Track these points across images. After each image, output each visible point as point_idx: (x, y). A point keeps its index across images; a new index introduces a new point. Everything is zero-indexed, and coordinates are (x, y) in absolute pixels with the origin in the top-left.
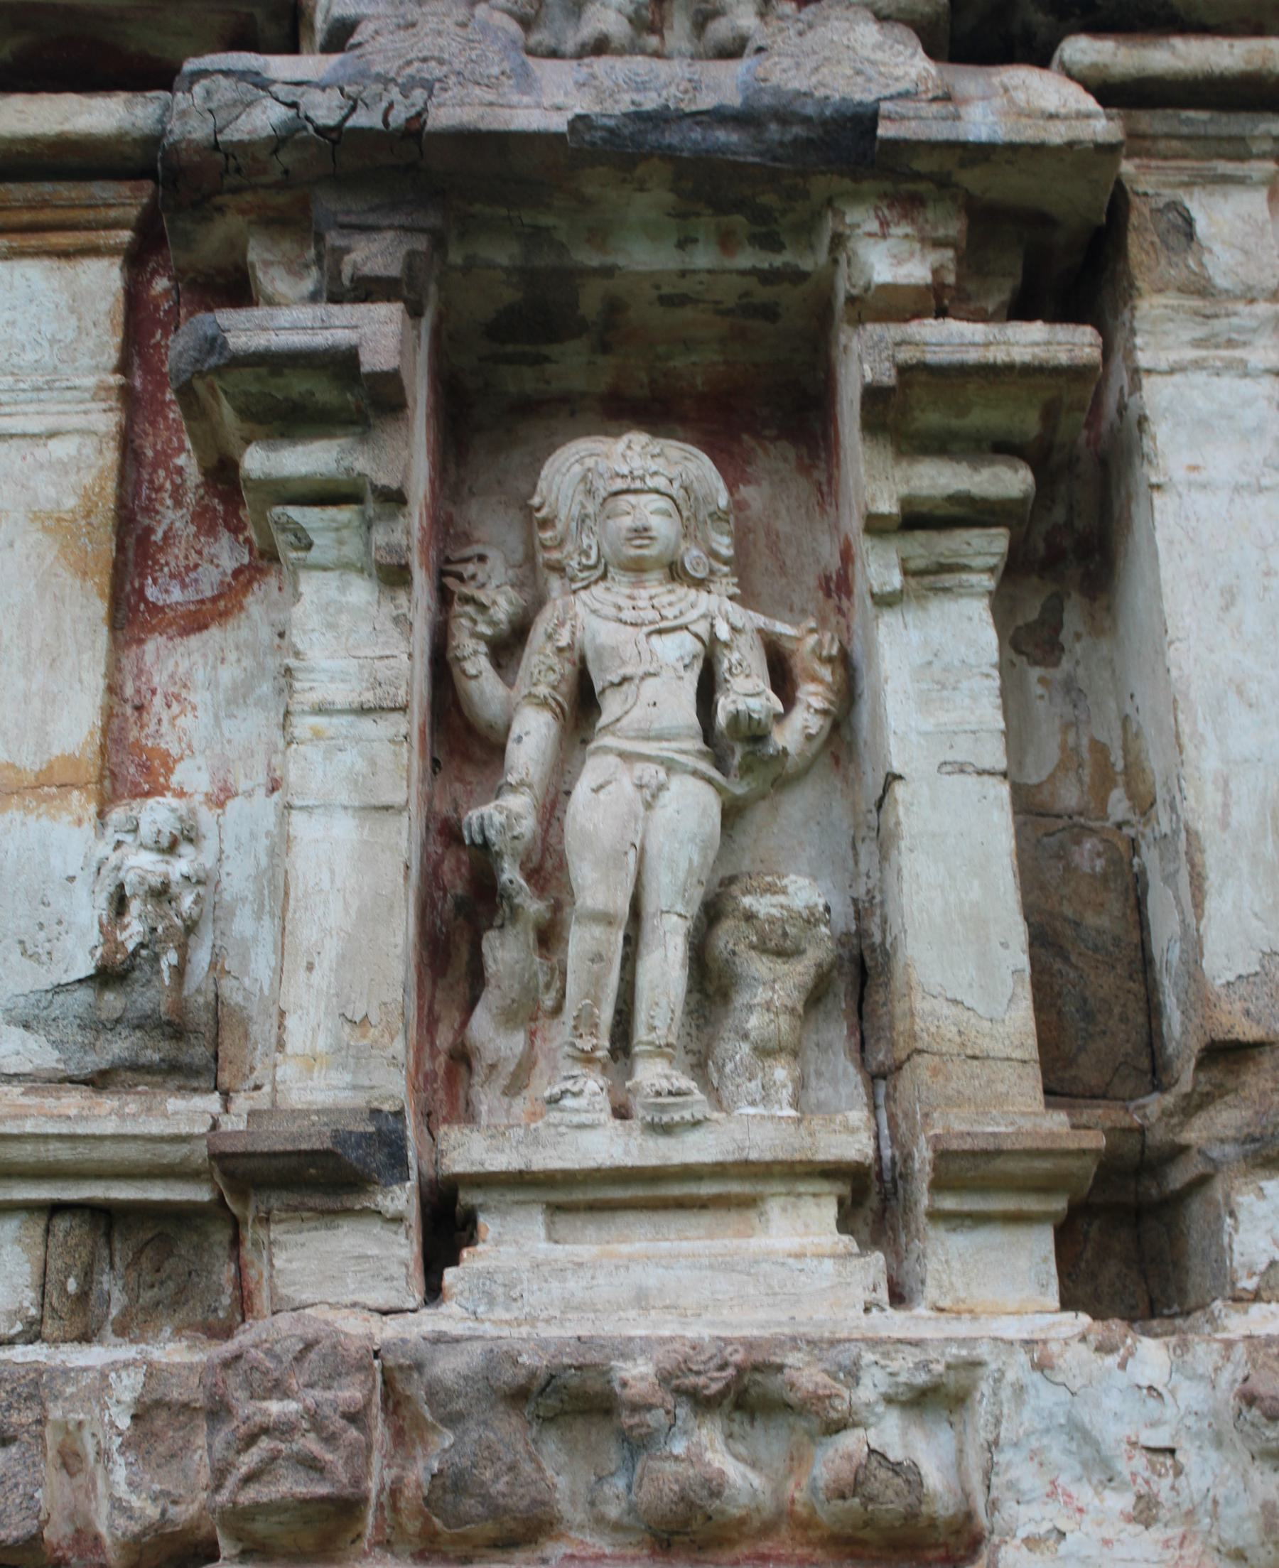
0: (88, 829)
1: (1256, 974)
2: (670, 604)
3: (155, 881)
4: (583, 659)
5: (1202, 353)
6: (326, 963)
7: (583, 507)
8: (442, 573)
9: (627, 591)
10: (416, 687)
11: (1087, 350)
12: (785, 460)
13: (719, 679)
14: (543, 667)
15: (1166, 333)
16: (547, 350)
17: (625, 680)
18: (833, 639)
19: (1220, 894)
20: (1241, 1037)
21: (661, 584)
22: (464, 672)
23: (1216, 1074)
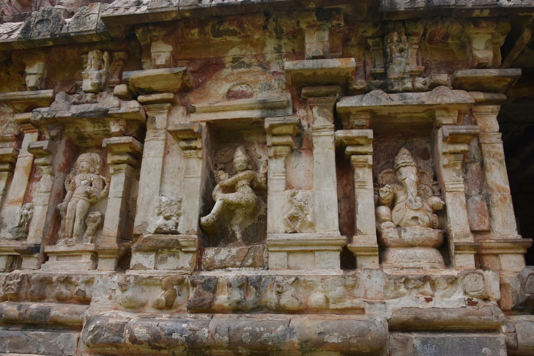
0: (20, 208)
3: (25, 214)
6: (35, 226)
16: (87, 141)
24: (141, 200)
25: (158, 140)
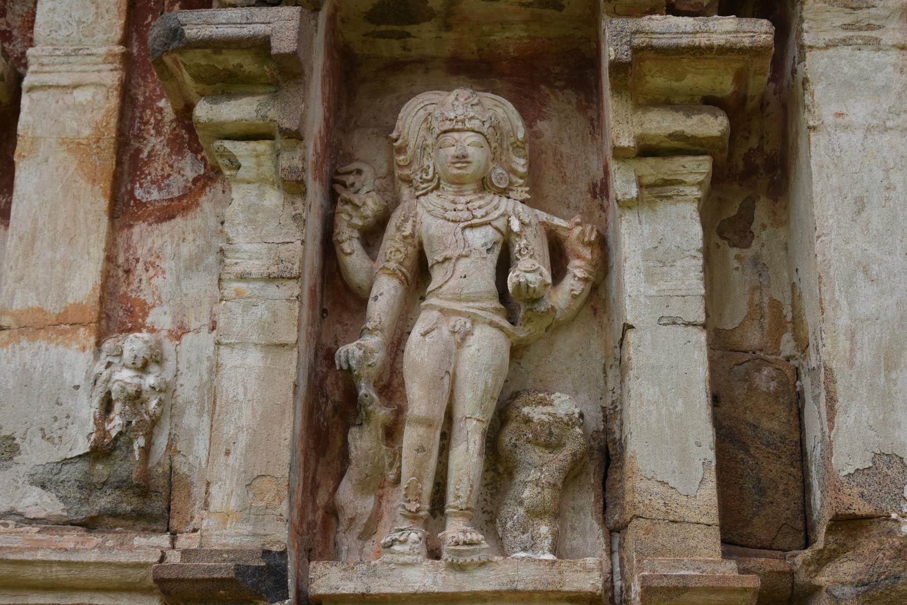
0: (89, 354)
1: (869, 468)
2: (480, 207)
3: (131, 390)
4: (421, 244)
5: (850, 34)
6: (238, 450)
7: (425, 140)
8: (333, 181)
9: (451, 197)
10: (308, 262)
11: (764, 36)
12: (569, 103)
13: (513, 257)
14: (393, 249)
15: (824, 20)
16: (409, 29)
17: (446, 259)
18: (592, 229)
19: (846, 412)
20: (857, 512)
21: (475, 192)
22: (342, 250)
23: (841, 537)
24: (844, 343)
25: (876, 44)
